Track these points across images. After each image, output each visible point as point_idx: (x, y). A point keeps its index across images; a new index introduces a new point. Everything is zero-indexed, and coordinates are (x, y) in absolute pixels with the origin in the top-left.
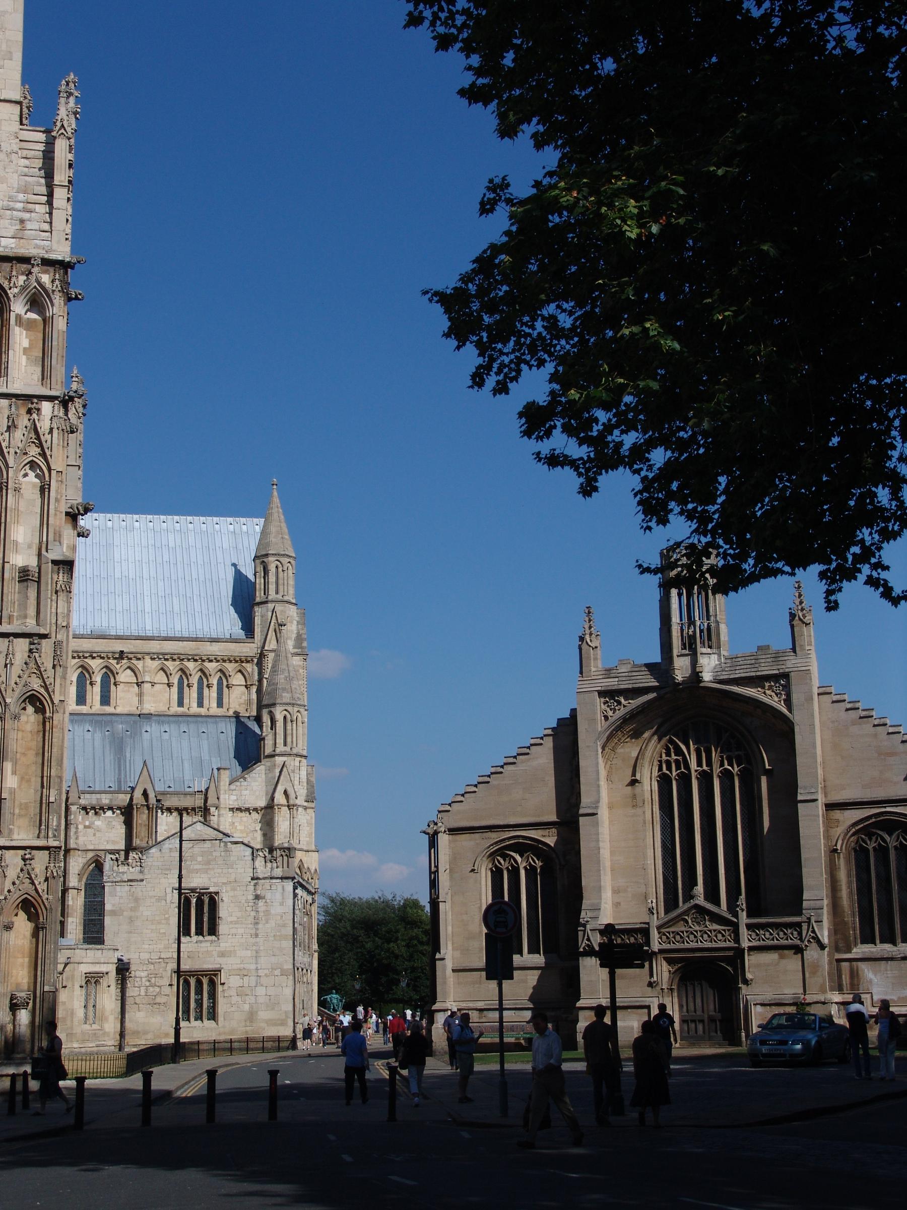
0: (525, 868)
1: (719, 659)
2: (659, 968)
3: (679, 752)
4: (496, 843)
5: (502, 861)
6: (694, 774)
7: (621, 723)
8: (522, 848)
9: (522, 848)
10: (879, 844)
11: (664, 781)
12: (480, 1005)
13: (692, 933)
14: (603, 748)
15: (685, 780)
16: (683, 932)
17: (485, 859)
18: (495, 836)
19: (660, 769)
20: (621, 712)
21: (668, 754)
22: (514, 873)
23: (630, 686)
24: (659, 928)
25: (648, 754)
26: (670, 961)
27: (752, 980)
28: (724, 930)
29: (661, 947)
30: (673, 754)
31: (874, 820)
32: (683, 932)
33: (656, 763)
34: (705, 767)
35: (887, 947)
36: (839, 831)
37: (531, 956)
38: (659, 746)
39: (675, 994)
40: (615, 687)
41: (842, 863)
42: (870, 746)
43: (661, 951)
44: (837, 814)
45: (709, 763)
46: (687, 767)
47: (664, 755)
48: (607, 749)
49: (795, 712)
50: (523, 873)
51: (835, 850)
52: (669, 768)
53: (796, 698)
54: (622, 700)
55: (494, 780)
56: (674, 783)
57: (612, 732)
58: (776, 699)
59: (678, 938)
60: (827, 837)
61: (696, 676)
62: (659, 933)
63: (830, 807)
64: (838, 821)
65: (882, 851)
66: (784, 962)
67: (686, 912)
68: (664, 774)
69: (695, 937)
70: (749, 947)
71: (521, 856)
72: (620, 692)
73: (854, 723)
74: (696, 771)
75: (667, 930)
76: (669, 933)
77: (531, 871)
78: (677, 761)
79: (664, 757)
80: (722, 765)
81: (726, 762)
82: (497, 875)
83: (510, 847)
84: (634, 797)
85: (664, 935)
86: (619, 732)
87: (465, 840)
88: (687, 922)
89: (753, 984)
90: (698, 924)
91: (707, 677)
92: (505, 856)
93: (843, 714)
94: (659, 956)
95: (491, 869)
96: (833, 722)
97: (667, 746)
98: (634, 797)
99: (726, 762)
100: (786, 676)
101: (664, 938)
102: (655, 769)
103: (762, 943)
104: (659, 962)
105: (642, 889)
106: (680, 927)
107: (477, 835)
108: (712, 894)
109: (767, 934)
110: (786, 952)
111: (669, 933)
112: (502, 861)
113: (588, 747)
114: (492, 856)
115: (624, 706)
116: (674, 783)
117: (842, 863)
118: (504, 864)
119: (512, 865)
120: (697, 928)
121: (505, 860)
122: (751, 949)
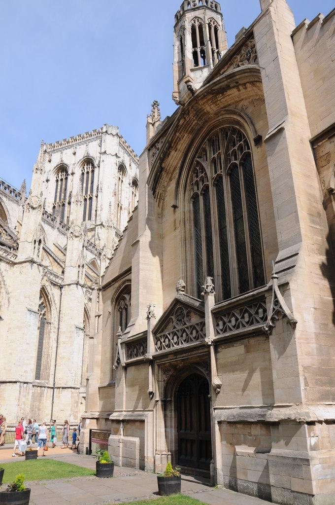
4: (118, 289)
7: (161, 164)
18: (117, 285)
27: (219, 387)
57: (156, 174)
66: (250, 356)
86: (163, 173)
109: (233, 319)
110: (252, 341)
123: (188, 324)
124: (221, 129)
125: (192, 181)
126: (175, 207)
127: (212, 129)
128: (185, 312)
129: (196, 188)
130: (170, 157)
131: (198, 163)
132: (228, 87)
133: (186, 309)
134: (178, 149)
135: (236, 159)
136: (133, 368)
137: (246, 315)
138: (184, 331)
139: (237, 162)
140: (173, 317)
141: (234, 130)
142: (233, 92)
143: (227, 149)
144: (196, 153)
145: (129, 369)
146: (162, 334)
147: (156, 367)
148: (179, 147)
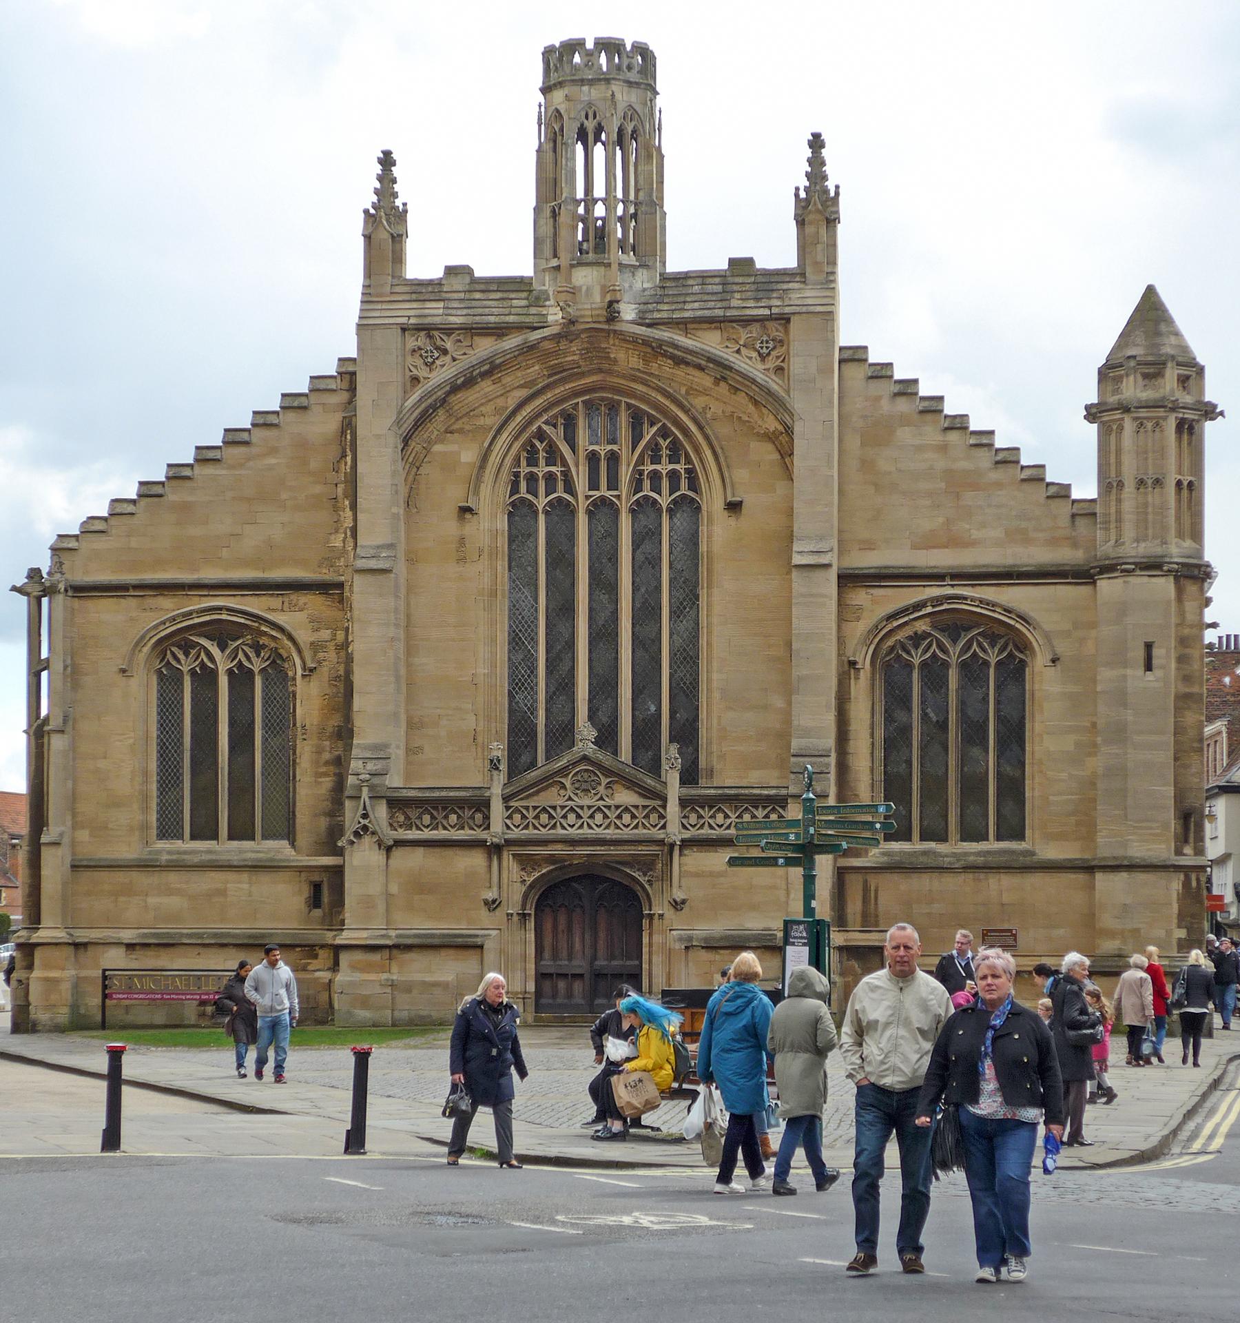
0: (230, 672)
1: (651, 279)
3: (553, 455)
5: (181, 656)
6: (582, 506)
7: (448, 394)
8: (222, 633)
9: (222, 633)
10: (934, 655)
11: (520, 511)
12: (128, 936)
13: (572, 809)
14: (406, 441)
15: (562, 511)
16: (554, 808)
17: (145, 650)
18: (169, 606)
19: (515, 489)
20: (444, 372)
21: (532, 461)
22: (205, 678)
23: (469, 320)
24: (506, 799)
25: (494, 459)
26: (526, 862)
28: (636, 807)
30: (542, 462)
31: (929, 610)
32: (554, 808)
33: (505, 476)
34: (608, 494)
35: (932, 845)
36: (859, 628)
37: (235, 843)
38: (517, 445)
39: (531, 924)
40: (437, 320)
41: (860, 690)
42: (931, 468)
43: (509, 843)
44: (860, 597)
45: (613, 484)
46: (570, 488)
47: (524, 463)
48: (412, 444)
49: (795, 394)
50: (223, 682)
51: (853, 664)
52: (533, 491)
53: (796, 366)
54: (449, 345)
55: (174, 496)
56: (542, 518)
57: (426, 410)
58: (760, 366)
59: (544, 818)
60: (841, 641)
61: (611, 312)
62: (508, 808)
63: (848, 580)
64: (860, 608)
65: (934, 673)
67: (563, 772)
68: (523, 500)
69: (579, 817)
70: (682, 841)
71: (222, 648)
72: (448, 331)
73: (905, 421)
74: (587, 497)
75: (524, 803)
76: (527, 808)
77: (241, 678)
78: (550, 478)
79: (524, 469)
80: (638, 488)
81: (647, 484)
82: (169, 681)
83: (202, 629)
84: (462, 541)
85: (517, 810)
86: (441, 412)
87: (106, 611)
88: (564, 787)
89: (686, 907)
91: (628, 312)
92: (187, 647)
93: (885, 405)
94: (505, 854)
95: (159, 672)
96: (864, 417)
97: (533, 446)
98: (462, 541)
99: (647, 484)
100: (785, 320)
101: (517, 817)
102: (504, 489)
103: (706, 831)
104: (505, 863)
105: (470, 722)
106: (551, 797)
107: (132, 602)
108: (607, 738)
109: (720, 817)
111: (527, 808)
112: (181, 656)
113: (378, 436)
114: (162, 647)
115: (454, 359)
116: (542, 518)
117: (860, 690)
118: (186, 665)
119: (202, 664)
120: (586, 801)
121: (187, 654)
122: (686, 844)
123: (609, 802)
124: (629, 406)
125: (517, 461)
126: (465, 510)
127: (602, 389)
128: (604, 781)
129: (523, 486)
130: (477, 388)
131: (541, 435)
132: (701, 368)
133: (607, 776)
134: (504, 382)
135: (656, 489)
136: (420, 851)
137: (747, 817)
139: (664, 501)
141: (664, 432)
142: (705, 380)
143: (640, 461)
144: (546, 410)
145: (397, 853)
146: (531, 803)
147: (507, 857)
148: (507, 380)
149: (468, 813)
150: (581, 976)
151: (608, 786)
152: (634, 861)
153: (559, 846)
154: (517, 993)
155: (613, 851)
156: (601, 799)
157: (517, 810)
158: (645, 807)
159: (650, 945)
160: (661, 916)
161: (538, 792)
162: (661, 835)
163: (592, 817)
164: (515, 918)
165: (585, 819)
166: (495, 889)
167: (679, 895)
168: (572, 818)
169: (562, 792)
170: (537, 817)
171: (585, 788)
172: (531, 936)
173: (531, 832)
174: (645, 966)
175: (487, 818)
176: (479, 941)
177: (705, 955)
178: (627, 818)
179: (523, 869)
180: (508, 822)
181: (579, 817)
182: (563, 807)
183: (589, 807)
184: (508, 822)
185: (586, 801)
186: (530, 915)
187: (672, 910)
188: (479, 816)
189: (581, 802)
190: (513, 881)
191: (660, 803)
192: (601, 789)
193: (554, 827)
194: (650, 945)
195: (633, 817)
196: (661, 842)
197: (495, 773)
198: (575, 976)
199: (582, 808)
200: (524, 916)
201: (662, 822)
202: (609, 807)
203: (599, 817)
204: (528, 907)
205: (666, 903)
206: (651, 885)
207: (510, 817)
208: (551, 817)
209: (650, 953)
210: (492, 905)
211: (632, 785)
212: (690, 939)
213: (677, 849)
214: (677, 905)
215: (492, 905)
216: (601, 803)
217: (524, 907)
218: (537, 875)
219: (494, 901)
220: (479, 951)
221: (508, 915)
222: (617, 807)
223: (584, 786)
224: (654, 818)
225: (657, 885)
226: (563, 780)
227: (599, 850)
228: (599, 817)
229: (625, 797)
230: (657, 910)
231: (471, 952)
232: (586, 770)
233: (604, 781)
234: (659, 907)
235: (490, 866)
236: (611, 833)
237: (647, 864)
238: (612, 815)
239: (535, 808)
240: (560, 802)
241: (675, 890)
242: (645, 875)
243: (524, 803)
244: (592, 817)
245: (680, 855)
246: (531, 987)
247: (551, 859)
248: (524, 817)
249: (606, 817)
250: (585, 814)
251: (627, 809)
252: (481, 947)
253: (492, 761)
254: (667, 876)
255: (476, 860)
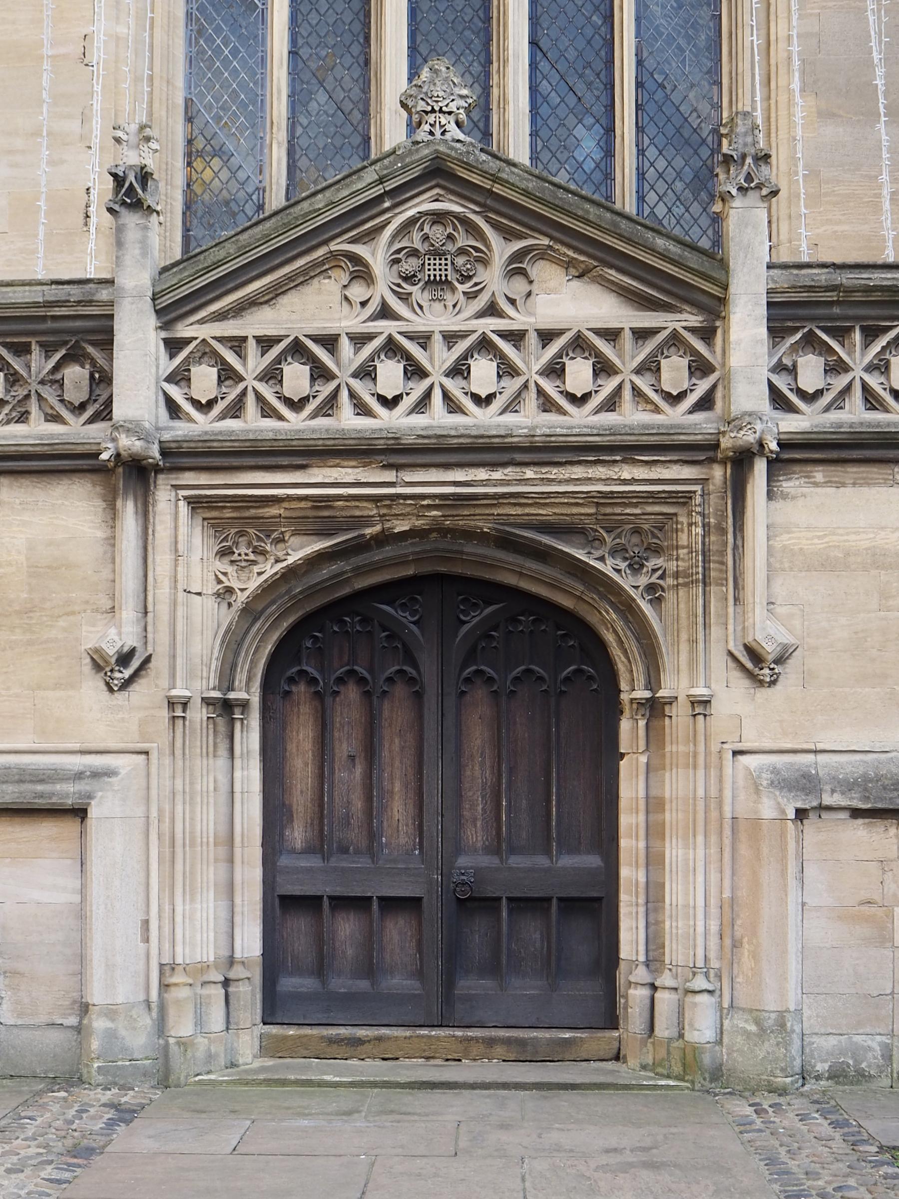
2: (161, 562)
13: (391, 348)
24: (169, 312)
26: (234, 523)
28: (611, 335)
29: (180, 430)
32: (330, 342)
39: (250, 738)
43: (178, 458)
59: (296, 378)
62: (173, 346)
69: (415, 371)
75: (230, 328)
76: (238, 344)
85: (206, 353)
88: (362, 272)
89: (790, 673)
90: (438, 284)
94: (164, 497)
101: (205, 379)
103: (854, 415)
106: (318, 307)
122: (796, 454)
123: (517, 320)
128: (501, 250)
133: (509, 235)
138: (484, 345)
140: (376, 255)
149: (39, 364)
150: (413, 904)
151: (516, 268)
152: (606, 518)
153: (347, 473)
154: (204, 968)
155: (530, 479)
156: (492, 310)
157: (206, 353)
158: (641, 335)
159: (654, 805)
160: (700, 705)
161: (275, 293)
162: (703, 424)
163: (459, 370)
164: (198, 714)
165: (437, 376)
166: (129, 613)
167: (769, 634)
168: (390, 375)
169: (358, 292)
170: (272, 375)
171: (434, 271)
172: (250, 776)
173: (252, 424)
174: (631, 874)
175: (102, 379)
176: (67, 792)
177: (860, 833)
178: (579, 375)
179: (224, 553)
180: (175, 392)
181: (415, 371)
182: (360, 340)
183: (451, 338)
184: (175, 392)
185: (436, 318)
186: (244, 705)
187: (741, 683)
188: (76, 375)
189: (419, 324)
190: (189, 589)
191: (695, 320)
192: (493, 279)
193: (330, 405)
194: (654, 805)
195: (603, 368)
196: (703, 451)
197: (131, 219)
198: (390, 904)
199: (424, 340)
200: (226, 709)
201: (703, 386)
202: (516, 337)
203: (483, 371)
204: (241, 678)
205: (718, 660)
206: (657, 602)
207: (180, 377)
208: (320, 373)
209: (654, 832)
210: (122, 669)
211: (595, 253)
212: (806, 783)
213: (760, 466)
214: (757, 665)
215: (122, 669)
216: (490, 324)
217: (227, 680)
218: (270, 569)
219: (125, 659)
220: (70, 827)
221: (171, 704)
222: (546, 337)
223: (434, 268)
224: (674, 371)
225: (679, 602)
226: (359, 249)
227: (479, 479)
228: (483, 371)
229: (569, 302)
230: (675, 684)
231: (47, 828)
232: (438, 217)
233: (501, 250)
234: (694, 670)
235: (112, 541)
236: (528, 421)
237: (644, 531)
238: (532, 361)
239: (266, 343)
240: (349, 321)
241: (758, 614)
242: (636, 567)
243: (230, 328)
244: (459, 370)
245: (770, 495)
246: (250, 942)
247: (319, 515)
248: (227, 374)
249: (507, 370)
250: (437, 360)
251: (579, 344)
252: (80, 813)
253: (118, 180)
254: (720, 566)
255: (69, 514)
